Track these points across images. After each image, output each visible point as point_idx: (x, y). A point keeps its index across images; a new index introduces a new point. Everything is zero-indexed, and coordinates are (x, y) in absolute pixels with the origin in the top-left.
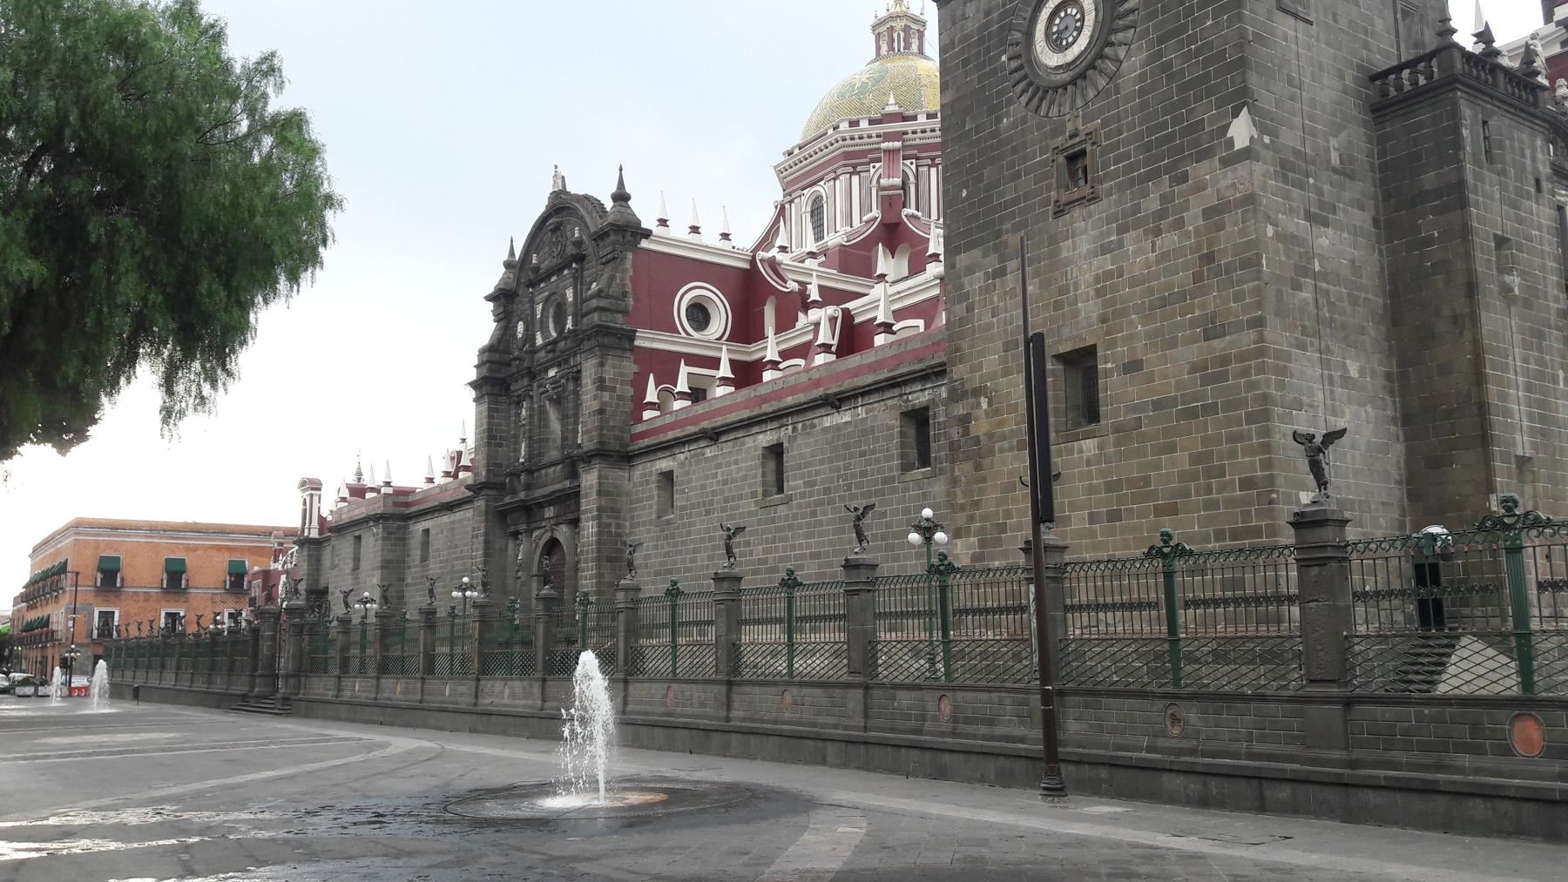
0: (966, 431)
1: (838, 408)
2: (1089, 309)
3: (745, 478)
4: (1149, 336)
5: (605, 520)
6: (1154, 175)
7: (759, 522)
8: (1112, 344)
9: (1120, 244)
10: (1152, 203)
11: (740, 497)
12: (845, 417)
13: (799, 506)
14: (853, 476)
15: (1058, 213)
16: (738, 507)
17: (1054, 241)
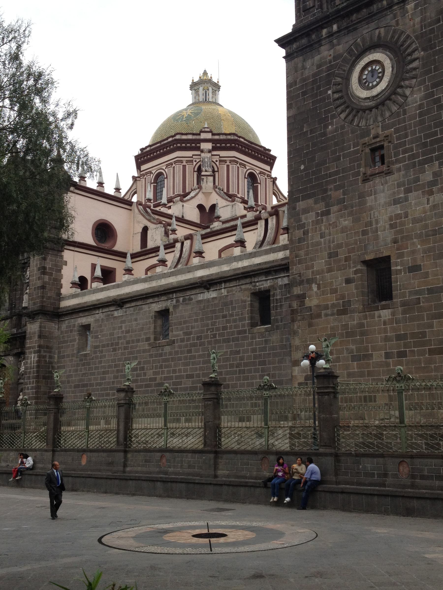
0: (302, 303)
1: (208, 289)
2: (386, 235)
3: (142, 329)
4: (425, 252)
5: (43, 353)
6: (430, 160)
7: (151, 356)
8: (401, 256)
9: (406, 199)
10: (428, 176)
11: (138, 341)
12: (212, 294)
13: (180, 347)
14: (218, 329)
15: (366, 180)
16: (137, 346)
17: (362, 196)
